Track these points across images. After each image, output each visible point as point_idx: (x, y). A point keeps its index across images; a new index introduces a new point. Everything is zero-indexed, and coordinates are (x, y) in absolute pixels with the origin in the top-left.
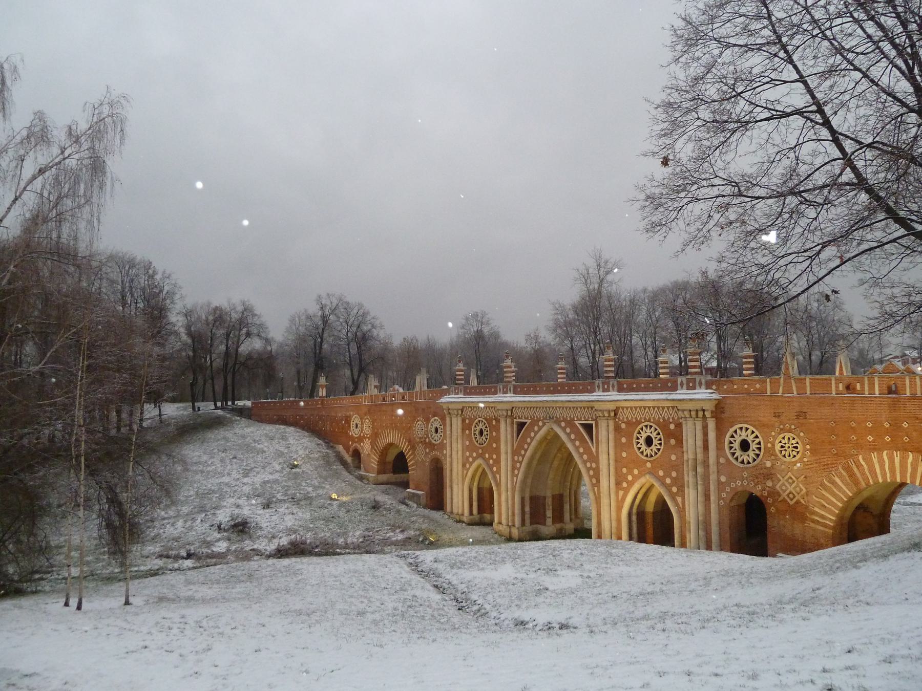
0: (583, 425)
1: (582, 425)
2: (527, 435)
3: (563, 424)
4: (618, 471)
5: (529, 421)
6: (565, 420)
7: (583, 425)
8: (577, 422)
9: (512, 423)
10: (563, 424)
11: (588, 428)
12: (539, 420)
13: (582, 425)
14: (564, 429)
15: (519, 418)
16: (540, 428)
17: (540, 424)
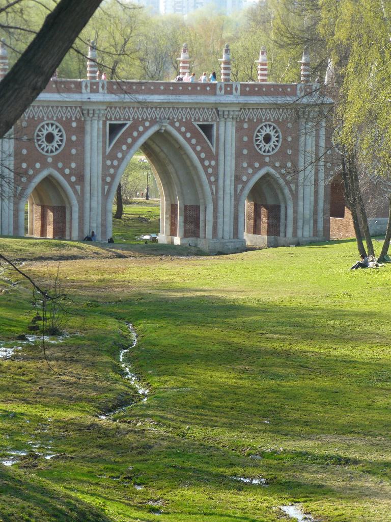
0: (201, 126)
1: (200, 126)
2: (122, 141)
3: (177, 124)
4: (238, 165)
5: (129, 123)
6: (180, 121)
7: (201, 126)
8: (195, 124)
9: (104, 123)
10: (177, 124)
11: (207, 129)
12: (144, 120)
13: (200, 126)
14: (178, 130)
15: (116, 119)
16: (146, 129)
17: (147, 124)
